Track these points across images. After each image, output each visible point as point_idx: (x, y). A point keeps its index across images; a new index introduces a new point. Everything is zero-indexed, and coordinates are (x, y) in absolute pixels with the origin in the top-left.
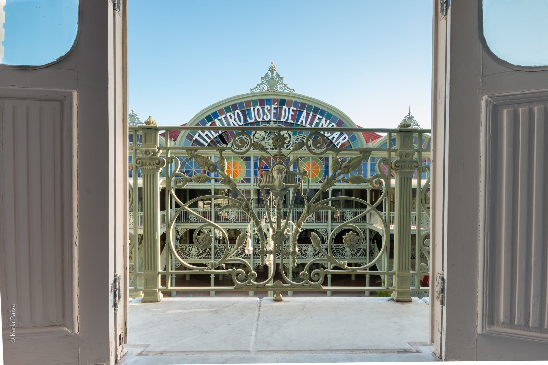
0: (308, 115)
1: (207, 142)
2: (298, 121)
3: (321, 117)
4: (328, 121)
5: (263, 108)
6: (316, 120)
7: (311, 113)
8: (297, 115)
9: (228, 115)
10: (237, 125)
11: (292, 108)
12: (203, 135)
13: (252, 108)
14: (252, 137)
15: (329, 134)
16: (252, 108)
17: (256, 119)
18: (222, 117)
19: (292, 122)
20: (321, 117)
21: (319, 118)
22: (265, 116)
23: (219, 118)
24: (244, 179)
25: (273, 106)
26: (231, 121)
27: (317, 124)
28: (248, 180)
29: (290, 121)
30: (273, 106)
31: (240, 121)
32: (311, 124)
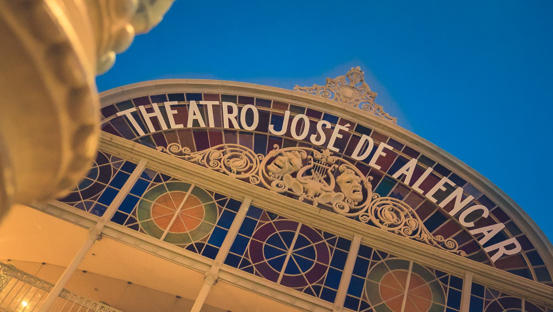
0: (418, 172)
1: (145, 129)
2: (393, 172)
3: (453, 184)
4: (470, 198)
5: (313, 125)
6: (440, 186)
7: (429, 170)
8: (393, 162)
9: (225, 105)
10: (236, 127)
11: (382, 145)
12: (147, 117)
13: (287, 114)
14: (266, 159)
15: (471, 224)
16: (287, 114)
17: (288, 133)
18: (210, 104)
19: (378, 168)
20: (453, 184)
21: (446, 185)
22: (313, 138)
23: (201, 103)
24: (200, 246)
25: (338, 127)
26: (226, 116)
27: (440, 196)
28: (211, 253)
29: (372, 164)
30: (338, 127)
31: (250, 123)
32: (426, 187)
